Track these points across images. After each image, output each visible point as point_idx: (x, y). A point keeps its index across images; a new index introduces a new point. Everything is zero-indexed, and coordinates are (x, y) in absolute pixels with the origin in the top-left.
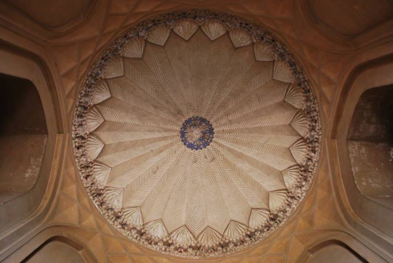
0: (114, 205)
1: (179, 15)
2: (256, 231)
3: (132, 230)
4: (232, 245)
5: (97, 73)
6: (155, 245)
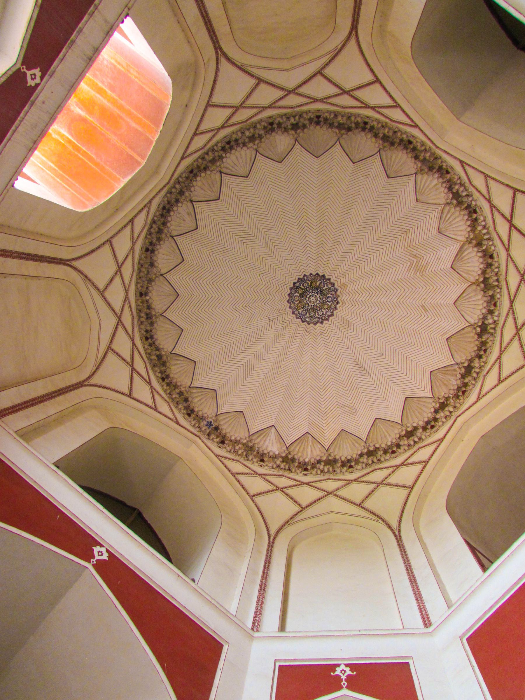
0: (317, 456)
1: (162, 215)
2: (485, 318)
3: (361, 460)
4: (477, 360)
5: (157, 356)
6: (400, 448)
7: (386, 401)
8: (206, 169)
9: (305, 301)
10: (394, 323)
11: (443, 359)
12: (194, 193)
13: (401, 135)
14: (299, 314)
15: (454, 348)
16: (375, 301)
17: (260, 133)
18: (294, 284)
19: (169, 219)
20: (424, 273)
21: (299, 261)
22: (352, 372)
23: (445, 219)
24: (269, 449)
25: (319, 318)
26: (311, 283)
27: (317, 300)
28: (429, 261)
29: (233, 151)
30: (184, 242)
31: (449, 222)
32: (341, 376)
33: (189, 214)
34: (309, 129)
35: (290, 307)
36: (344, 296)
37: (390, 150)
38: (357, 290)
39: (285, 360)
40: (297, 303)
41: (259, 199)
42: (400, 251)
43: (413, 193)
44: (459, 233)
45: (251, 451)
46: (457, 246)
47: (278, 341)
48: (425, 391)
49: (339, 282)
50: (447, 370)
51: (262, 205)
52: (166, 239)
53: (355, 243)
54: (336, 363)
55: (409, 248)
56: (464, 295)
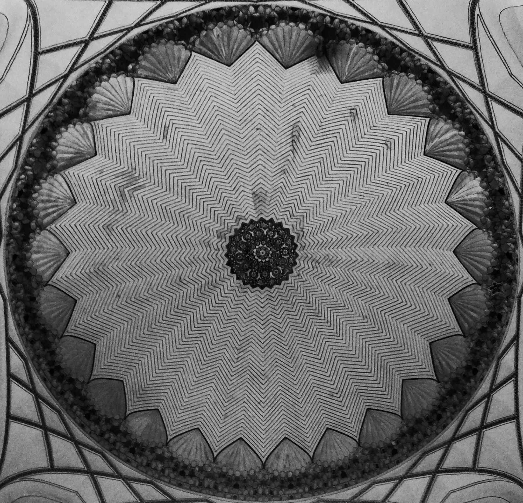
7: (311, 83)
8: (223, 475)
9: (271, 260)
10: (212, 149)
11: (201, 67)
12: (254, 468)
13: (29, 334)
14: (290, 257)
15: (177, 65)
16: (206, 189)
17: (149, 453)
18: (262, 288)
19: (297, 473)
20: (130, 170)
21: (235, 302)
22: (309, 148)
23: (58, 210)
24: (480, 189)
25: (278, 232)
26: (247, 270)
27: (260, 248)
28: (114, 177)
29: (187, 463)
30: (308, 440)
31: (56, 204)
32: (324, 156)
33: (278, 457)
34: (105, 415)
35: (292, 272)
36: (230, 225)
37: (51, 326)
38: (212, 217)
39: (355, 235)
40: (280, 268)
41: (209, 397)
42: (132, 215)
43: (65, 265)
44: (56, 184)
45: (498, 213)
46: (71, 171)
47: (339, 258)
48: (257, 51)
49: (221, 243)
50: (210, 50)
51: (211, 388)
52: (319, 463)
53: (167, 264)
54: (313, 173)
55: (121, 209)
56: (110, 113)
